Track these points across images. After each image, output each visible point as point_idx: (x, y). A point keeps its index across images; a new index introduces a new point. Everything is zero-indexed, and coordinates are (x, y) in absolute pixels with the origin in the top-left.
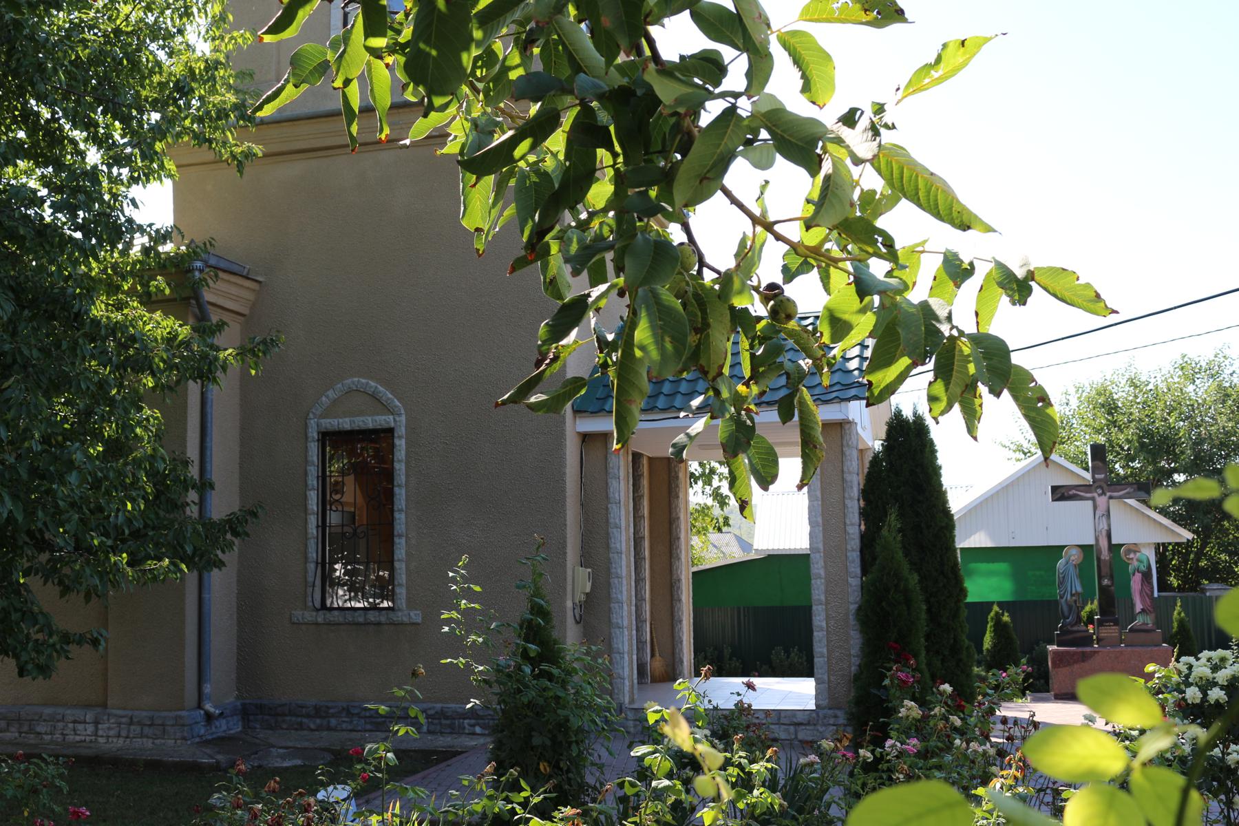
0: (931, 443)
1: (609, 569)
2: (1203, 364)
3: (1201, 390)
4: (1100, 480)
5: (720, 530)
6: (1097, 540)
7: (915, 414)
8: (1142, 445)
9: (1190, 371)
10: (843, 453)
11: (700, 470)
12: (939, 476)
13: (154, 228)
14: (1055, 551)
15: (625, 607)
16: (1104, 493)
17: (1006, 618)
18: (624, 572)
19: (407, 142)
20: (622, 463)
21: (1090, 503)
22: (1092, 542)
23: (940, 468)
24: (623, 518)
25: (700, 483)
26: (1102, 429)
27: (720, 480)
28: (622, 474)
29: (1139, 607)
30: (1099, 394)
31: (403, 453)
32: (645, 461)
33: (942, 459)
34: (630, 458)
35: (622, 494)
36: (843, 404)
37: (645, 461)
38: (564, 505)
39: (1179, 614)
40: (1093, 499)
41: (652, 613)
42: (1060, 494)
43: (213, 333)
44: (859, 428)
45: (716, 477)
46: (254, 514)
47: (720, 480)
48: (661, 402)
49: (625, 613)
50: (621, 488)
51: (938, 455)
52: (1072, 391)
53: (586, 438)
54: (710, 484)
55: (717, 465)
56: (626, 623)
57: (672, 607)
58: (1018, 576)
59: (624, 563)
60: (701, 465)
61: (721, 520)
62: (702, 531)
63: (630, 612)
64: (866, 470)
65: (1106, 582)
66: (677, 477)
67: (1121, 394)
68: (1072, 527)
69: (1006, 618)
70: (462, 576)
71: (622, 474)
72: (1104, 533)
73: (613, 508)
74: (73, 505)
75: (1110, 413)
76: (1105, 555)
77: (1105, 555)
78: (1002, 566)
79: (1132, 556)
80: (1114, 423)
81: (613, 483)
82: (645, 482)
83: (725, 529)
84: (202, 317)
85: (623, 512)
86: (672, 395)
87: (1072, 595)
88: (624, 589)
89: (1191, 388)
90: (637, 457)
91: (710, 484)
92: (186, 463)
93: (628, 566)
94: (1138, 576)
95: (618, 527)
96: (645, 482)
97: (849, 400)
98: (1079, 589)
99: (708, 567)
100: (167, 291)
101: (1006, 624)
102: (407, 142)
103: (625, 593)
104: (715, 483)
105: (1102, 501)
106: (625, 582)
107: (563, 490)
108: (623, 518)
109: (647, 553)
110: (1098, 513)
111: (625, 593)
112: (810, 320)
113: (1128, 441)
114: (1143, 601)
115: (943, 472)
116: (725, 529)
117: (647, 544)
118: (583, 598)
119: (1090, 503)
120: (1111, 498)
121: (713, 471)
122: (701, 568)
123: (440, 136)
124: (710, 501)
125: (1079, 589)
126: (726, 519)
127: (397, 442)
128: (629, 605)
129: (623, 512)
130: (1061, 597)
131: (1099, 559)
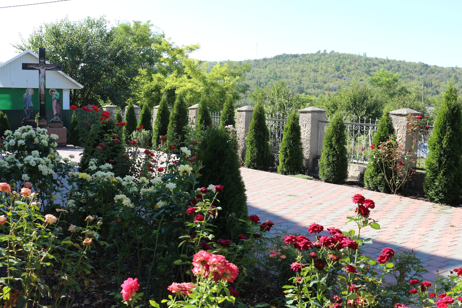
2: (96, 22)
3: (94, 31)
4: (42, 62)
6: (40, 86)
8: (68, 50)
9: (91, 24)
14: (24, 90)
17: (5, 116)
22: (38, 87)
29: (55, 113)
30: (53, 28)
39: (74, 116)
42: (25, 67)
52: (43, 26)
58: (13, 100)
65: (42, 103)
67: (63, 29)
68: (30, 81)
69: (5, 116)
72: (43, 83)
75: (57, 37)
76: (43, 92)
77: (43, 92)
78: (7, 96)
79: (53, 93)
80: (58, 41)
87: (29, 108)
89: (90, 30)
94: (55, 101)
98: (32, 105)
101: (5, 119)
113: (62, 48)
114: (57, 111)
120: (46, 69)
125: (32, 105)
130: (25, 108)
131: (40, 94)
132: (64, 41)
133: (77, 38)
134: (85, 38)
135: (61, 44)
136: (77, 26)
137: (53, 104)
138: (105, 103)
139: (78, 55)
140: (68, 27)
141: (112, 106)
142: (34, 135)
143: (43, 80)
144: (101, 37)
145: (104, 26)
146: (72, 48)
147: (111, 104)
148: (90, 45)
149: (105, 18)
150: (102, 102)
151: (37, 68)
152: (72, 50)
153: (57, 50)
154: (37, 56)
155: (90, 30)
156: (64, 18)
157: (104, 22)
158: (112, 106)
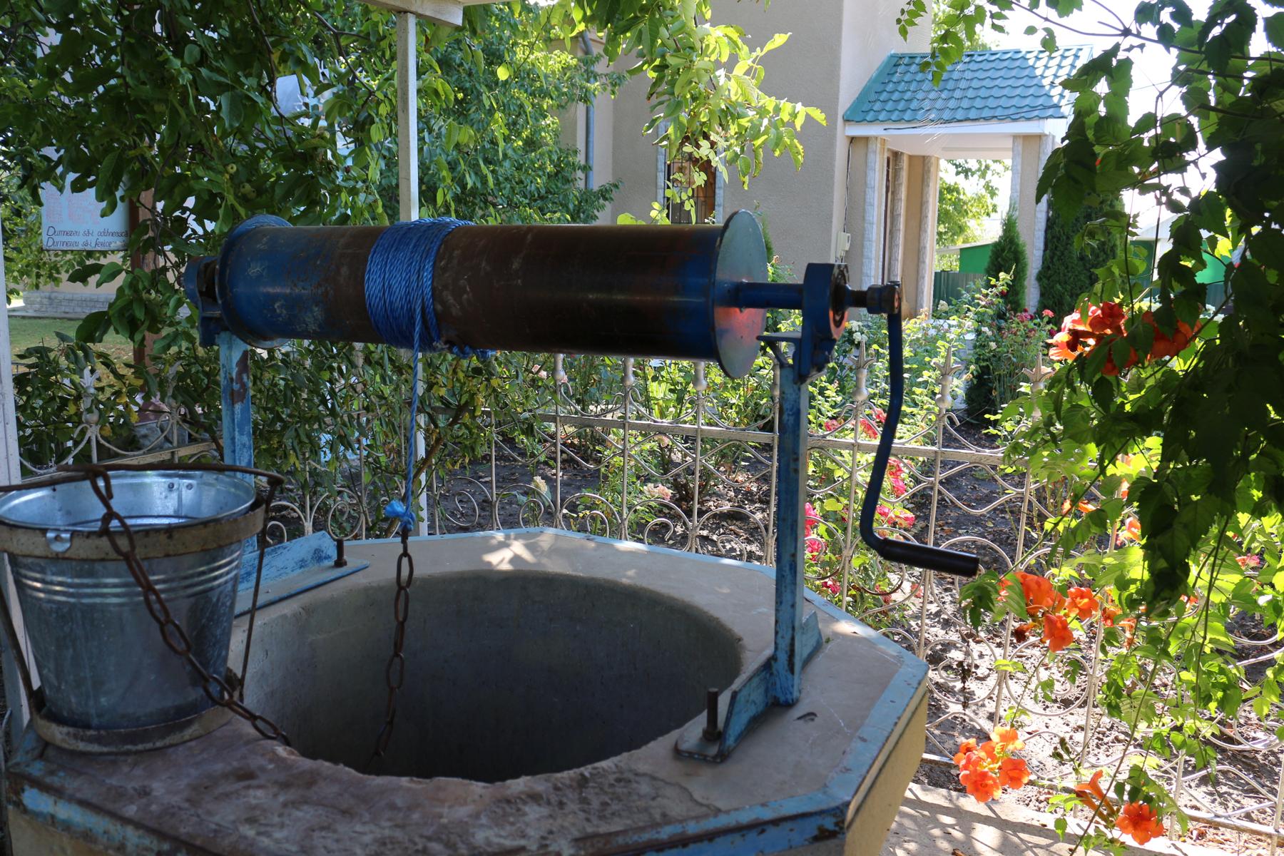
1: (863, 235)
5: (988, 215)
18: (874, 237)
32: (905, 159)
38: (832, 188)
41: (903, 271)
43: (593, 63)
46: (616, 186)
48: (907, 116)
53: (852, 140)
57: (918, 266)
60: (979, 162)
61: (990, 208)
63: (877, 266)
73: (869, 191)
74: (506, 179)
81: (870, 174)
83: (993, 215)
84: (587, 52)
86: (904, 111)
92: (576, 152)
93: (878, 234)
96: (904, 175)
104: (988, 178)
107: (832, 177)
109: (902, 227)
116: (993, 215)
117: (902, 219)
118: (843, 254)
121: (987, 167)
122: (974, 244)
124: (983, 192)
126: (995, 206)
128: (877, 261)
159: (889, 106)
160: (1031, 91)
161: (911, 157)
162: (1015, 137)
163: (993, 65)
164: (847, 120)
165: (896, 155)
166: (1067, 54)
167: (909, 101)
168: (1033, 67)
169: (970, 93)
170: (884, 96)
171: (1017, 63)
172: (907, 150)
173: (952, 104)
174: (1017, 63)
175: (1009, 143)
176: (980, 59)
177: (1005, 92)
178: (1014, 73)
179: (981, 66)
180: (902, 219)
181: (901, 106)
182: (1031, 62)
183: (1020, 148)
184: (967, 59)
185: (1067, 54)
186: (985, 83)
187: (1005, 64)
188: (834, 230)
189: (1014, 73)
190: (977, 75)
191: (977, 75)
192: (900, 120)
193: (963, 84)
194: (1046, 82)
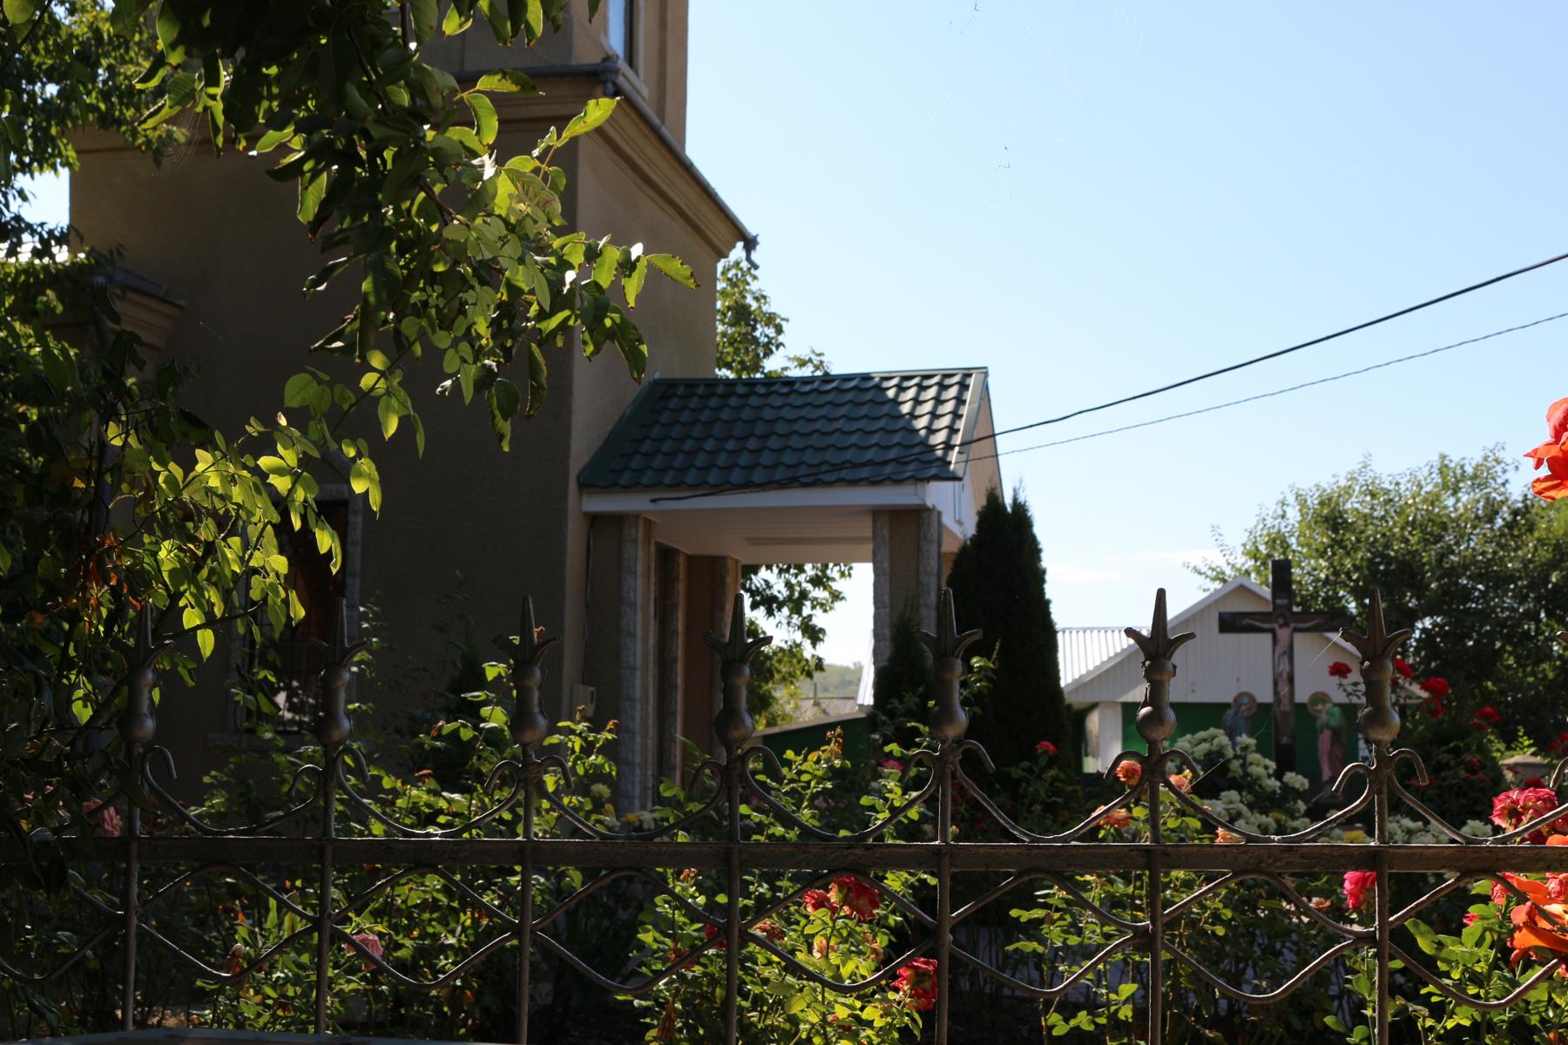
0: (1033, 541)
2: (1469, 470)
4: (1282, 606)
5: (809, 675)
7: (1015, 500)
9: (1451, 479)
10: (919, 549)
11: (785, 592)
12: (1043, 581)
13: (46, 228)
15: (638, 739)
16: (1286, 625)
19: (254, 153)
20: (640, 554)
21: (1268, 637)
23: (1044, 572)
24: (639, 624)
25: (786, 611)
26: (1325, 552)
27: (813, 607)
28: (640, 568)
30: (1322, 503)
31: (359, 532)
32: (681, 560)
33: (1048, 560)
34: (653, 549)
35: (639, 594)
36: (919, 486)
37: (681, 560)
40: (1272, 631)
42: (1231, 623)
44: (947, 520)
45: (808, 603)
47: (813, 607)
48: (691, 477)
49: (638, 747)
50: (640, 587)
51: (1043, 555)
52: (1291, 499)
53: (595, 520)
54: (799, 613)
55: (809, 587)
56: (638, 759)
59: (638, 681)
62: (788, 679)
64: (947, 571)
65: (1285, 740)
66: (723, 583)
67: (1353, 505)
70: (375, 613)
71: (640, 568)
72: (1285, 676)
75: (1336, 531)
79: (1320, 707)
80: (1340, 543)
82: (681, 587)
83: (817, 675)
85: (639, 617)
88: (638, 715)
89: (1450, 502)
90: (666, 555)
91: (800, 614)
94: (1326, 736)
95: (632, 635)
96: (681, 587)
97: (928, 479)
99: (794, 726)
100: (60, 308)
102: (254, 153)
103: (638, 720)
104: (806, 611)
105: (1283, 634)
106: (638, 707)
108: (639, 624)
109: (680, 680)
110: (1279, 650)
111: (638, 720)
112: (894, 382)
115: (1047, 577)
116: (817, 675)
117: (680, 667)
119: (1268, 637)
120: (1296, 630)
121: (804, 595)
123: (284, 149)
124: (798, 636)
127: (352, 518)
128: (645, 736)
129: (639, 617)
132: (1358, 540)
133: (1402, 529)
134: (1434, 527)
135: (1348, 554)
136: (1403, 488)
137: (1320, 744)
138: (1509, 748)
139: (1410, 586)
140: (1373, 496)
141: (1538, 759)
142: (1230, 753)
143: (1284, 666)
144: (1491, 520)
145: (1500, 481)
146: (1388, 564)
147: (1534, 754)
148: (1453, 552)
149: (1500, 455)
150: (1502, 746)
151: (1267, 626)
152: (1385, 573)
153: (1336, 573)
154: (1266, 592)
155: (1450, 502)
156: (1357, 467)
157: (1499, 468)
158: (1538, 759)
159: (657, 462)
160: (897, 438)
161: (691, 559)
162: (877, 513)
163: (829, 397)
164: (587, 484)
165: (666, 555)
166: (948, 382)
167: (692, 453)
168: (896, 403)
169: (788, 458)
170: (647, 446)
171: (869, 396)
172: (688, 545)
173: (766, 458)
174: (869, 396)
175: (865, 527)
176: (807, 388)
177: (854, 439)
178: (864, 410)
179: (810, 399)
180: (680, 667)
181: (679, 461)
182: (891, 393)
183: (886, 532)
184: (785, 390)
185: (948, 382)
186: (817, 426)
187: (849, 396)
188: (566, 681)
189: (864, 410)
190: (804, 413)
191: (804, 413)
192: (677, 485)
193: (781, 428)
194: (921, 423)
